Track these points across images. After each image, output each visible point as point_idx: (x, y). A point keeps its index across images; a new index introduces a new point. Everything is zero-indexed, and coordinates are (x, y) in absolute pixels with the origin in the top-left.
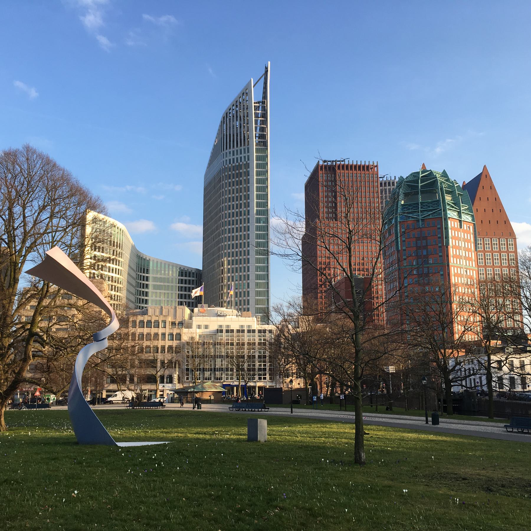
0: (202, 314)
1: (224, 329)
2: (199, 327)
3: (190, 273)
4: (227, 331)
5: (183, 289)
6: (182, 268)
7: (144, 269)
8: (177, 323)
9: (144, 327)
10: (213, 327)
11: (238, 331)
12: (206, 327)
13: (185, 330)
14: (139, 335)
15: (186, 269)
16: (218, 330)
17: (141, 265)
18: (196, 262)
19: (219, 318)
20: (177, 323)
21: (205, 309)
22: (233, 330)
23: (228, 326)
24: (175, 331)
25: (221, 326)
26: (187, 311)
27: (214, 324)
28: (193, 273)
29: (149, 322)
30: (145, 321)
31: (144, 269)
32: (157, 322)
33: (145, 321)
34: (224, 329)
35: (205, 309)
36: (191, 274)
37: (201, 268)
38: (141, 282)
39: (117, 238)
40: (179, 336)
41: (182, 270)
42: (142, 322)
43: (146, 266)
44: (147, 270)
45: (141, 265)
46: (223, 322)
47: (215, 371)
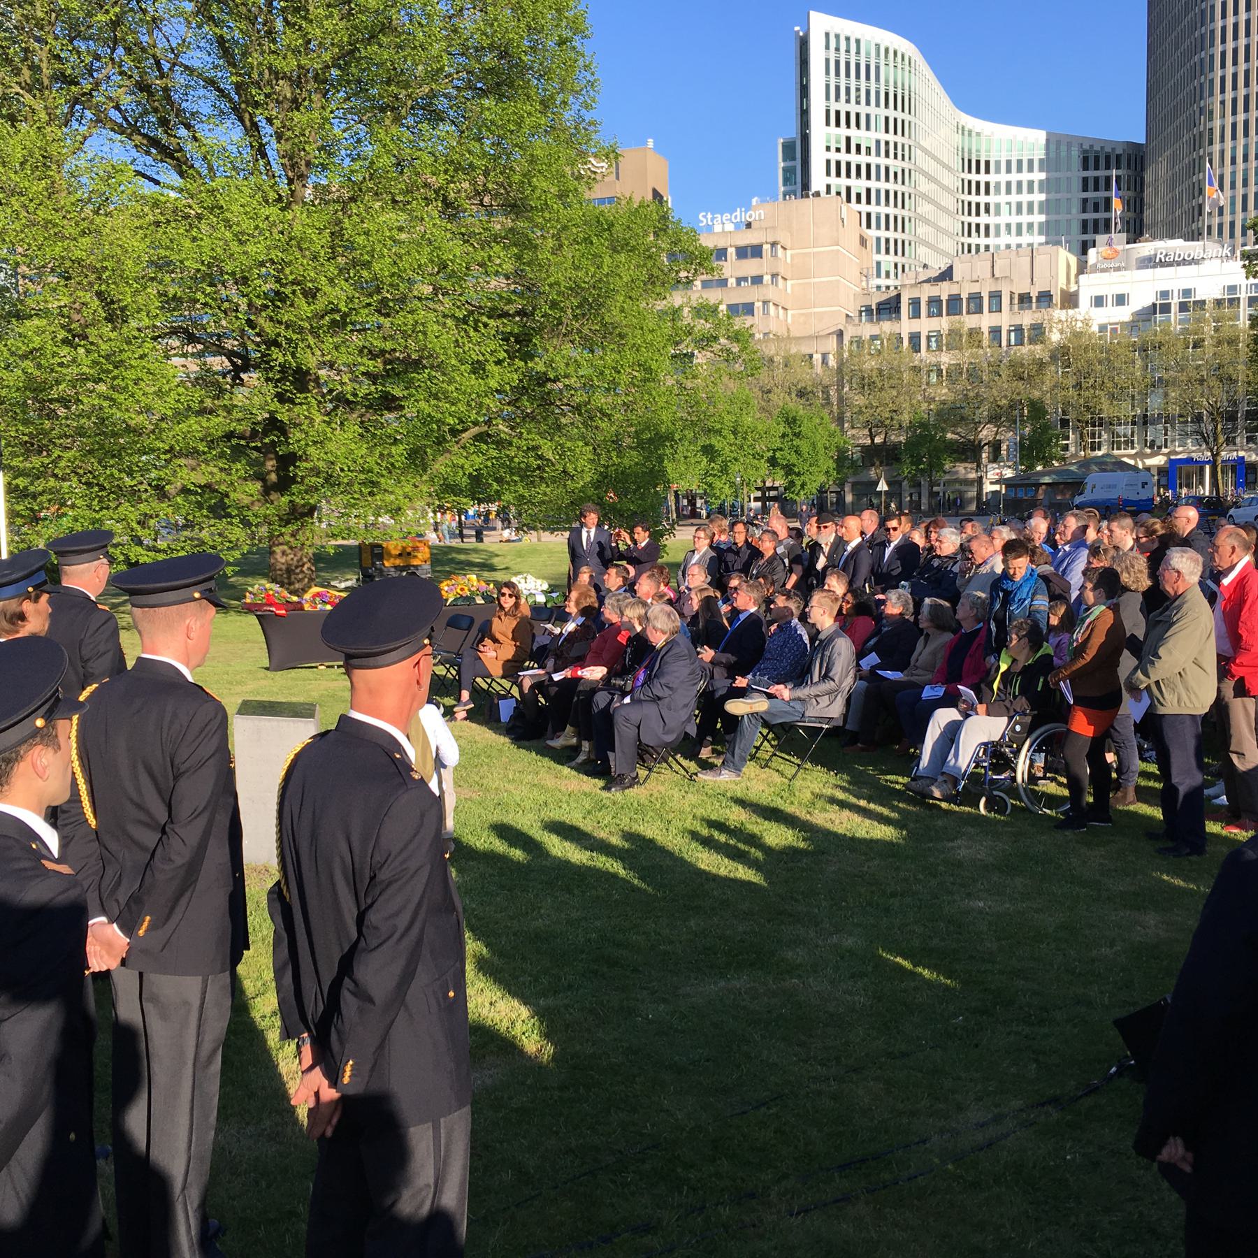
0: (1114, 265)
1: (1175, 301)
2: (1099, 301)
3: (1108, 158)
4: (1183, 307)
5: (1090, 206)
6: (1086, 147)
7: (978, 162)
8: (1034, 295)
9: (940, 315)
10: (1142, 298)
11: (1219, 303)
12: (1121, 300)
13: (1058, 314)
14: (929, 338)
15: (1097, 148)
16: (1154, 305)
17: (970, 150)
18: (1128, 126)
19: (1159, 270)
20: (1034, 295)
21: (1120, 248)
22: (1204, 302)
23: (1187, 292)
24: (1027, 319)
25: (1165, 294)
26: (1065, 257)
27: (1142, 288)
28: (1118, 157)
29: (954, 302)
30: (944, 298)
31: (978, 162)
32: (976, 299)
33: (944, 298)
34: (1175, 301)
35: (1120, 248)
36: (1113, 161)
37: (1142, 140)
38: (969, 198)
39: (887, 81)
40: (1038, 332)
41: (1085, 152)
42: (934, 301)
43: (974, 151)
44: (987, 163)
45: (970, 150)
46: (1173, 280)
47: (1145, 423)
